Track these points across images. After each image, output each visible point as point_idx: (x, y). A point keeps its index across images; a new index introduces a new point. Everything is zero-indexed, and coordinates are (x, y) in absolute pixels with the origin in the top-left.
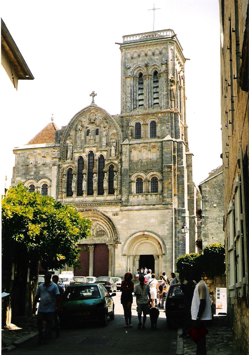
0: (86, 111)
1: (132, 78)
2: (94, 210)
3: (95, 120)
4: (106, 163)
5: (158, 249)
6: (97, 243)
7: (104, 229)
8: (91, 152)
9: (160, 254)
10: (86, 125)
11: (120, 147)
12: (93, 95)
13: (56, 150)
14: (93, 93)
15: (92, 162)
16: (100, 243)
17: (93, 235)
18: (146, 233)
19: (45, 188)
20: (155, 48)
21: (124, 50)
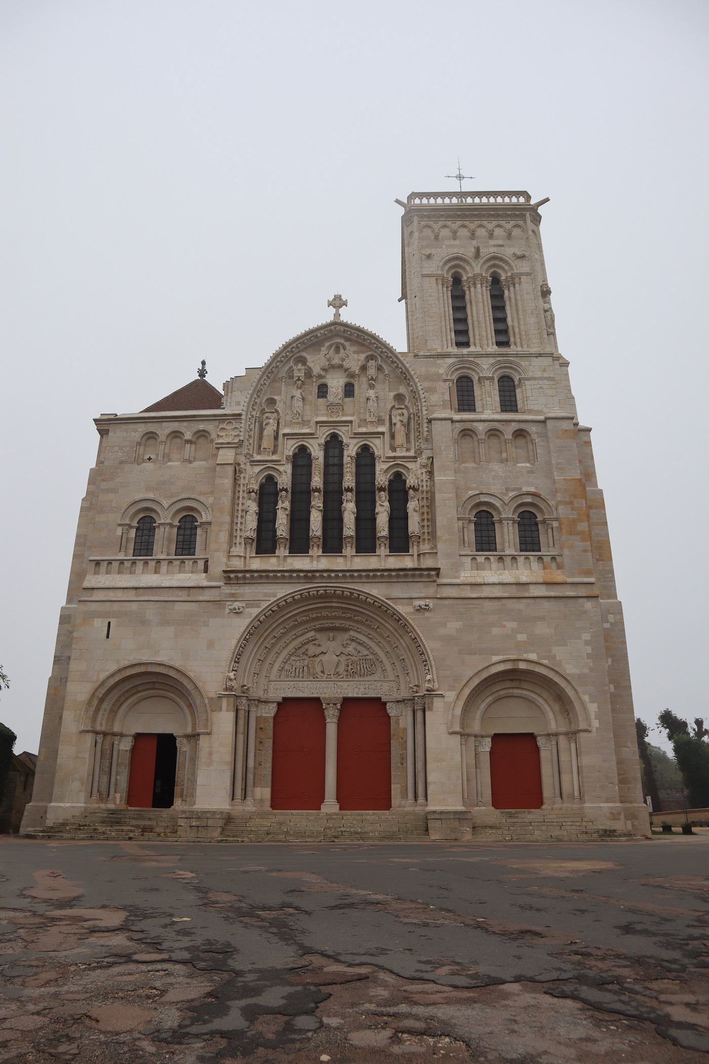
0: (319, 335)
1: (440, 282)
2: (352, 594)
3: (343, 360)
4: (380, 467)
5: (550, 715)
6: (350, 695)
7: (371, 657)
8: (334, 437)
9: (562, 729)
10: (316, 370)
11: (426, 425)
12: (338, 302)
13: (229, 427)
14: (338, 298)
15: (336, 462)
16: (360, 695)
17: (338, 674)
18: (522, 666)
19: (188, 526)
20: (495, 223)
21: (416, 218)
